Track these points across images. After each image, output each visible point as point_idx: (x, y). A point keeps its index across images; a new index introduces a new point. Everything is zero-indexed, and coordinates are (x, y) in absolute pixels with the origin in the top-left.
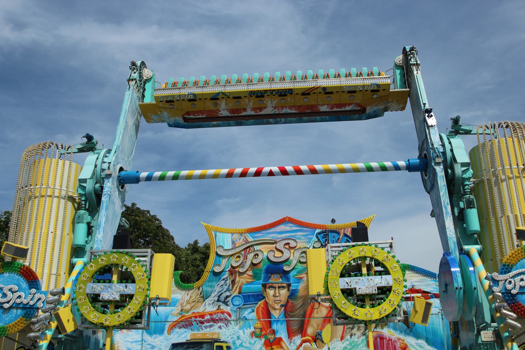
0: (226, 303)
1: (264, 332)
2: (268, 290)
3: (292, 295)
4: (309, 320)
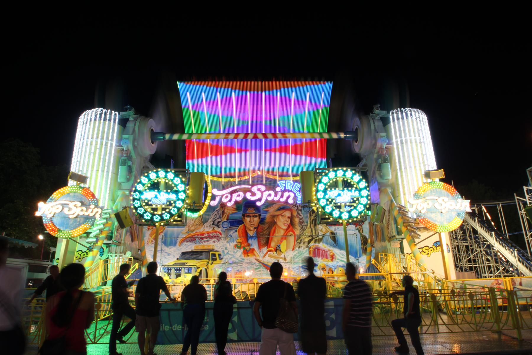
0: (218, 226)
1: (243, 245)
2: (246, 218)
3: (262, 221)
4: (272, 238)
